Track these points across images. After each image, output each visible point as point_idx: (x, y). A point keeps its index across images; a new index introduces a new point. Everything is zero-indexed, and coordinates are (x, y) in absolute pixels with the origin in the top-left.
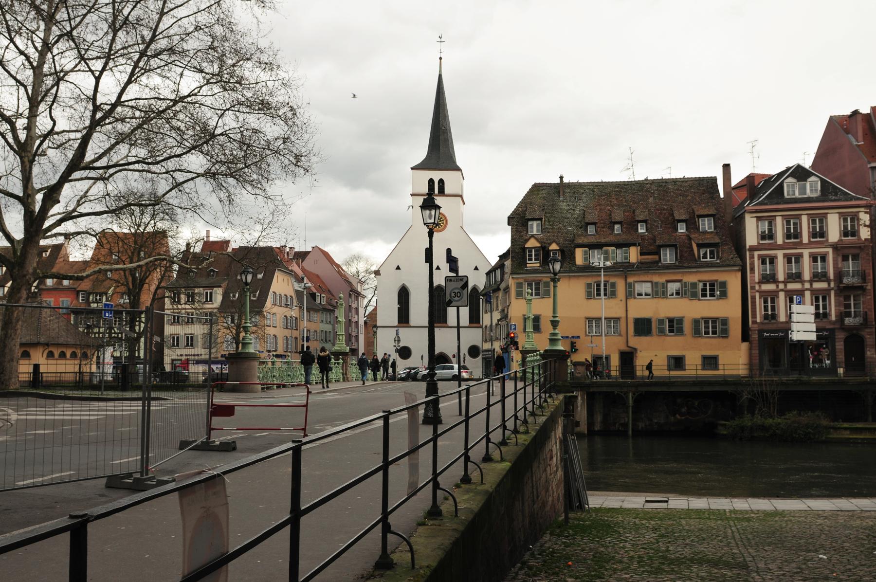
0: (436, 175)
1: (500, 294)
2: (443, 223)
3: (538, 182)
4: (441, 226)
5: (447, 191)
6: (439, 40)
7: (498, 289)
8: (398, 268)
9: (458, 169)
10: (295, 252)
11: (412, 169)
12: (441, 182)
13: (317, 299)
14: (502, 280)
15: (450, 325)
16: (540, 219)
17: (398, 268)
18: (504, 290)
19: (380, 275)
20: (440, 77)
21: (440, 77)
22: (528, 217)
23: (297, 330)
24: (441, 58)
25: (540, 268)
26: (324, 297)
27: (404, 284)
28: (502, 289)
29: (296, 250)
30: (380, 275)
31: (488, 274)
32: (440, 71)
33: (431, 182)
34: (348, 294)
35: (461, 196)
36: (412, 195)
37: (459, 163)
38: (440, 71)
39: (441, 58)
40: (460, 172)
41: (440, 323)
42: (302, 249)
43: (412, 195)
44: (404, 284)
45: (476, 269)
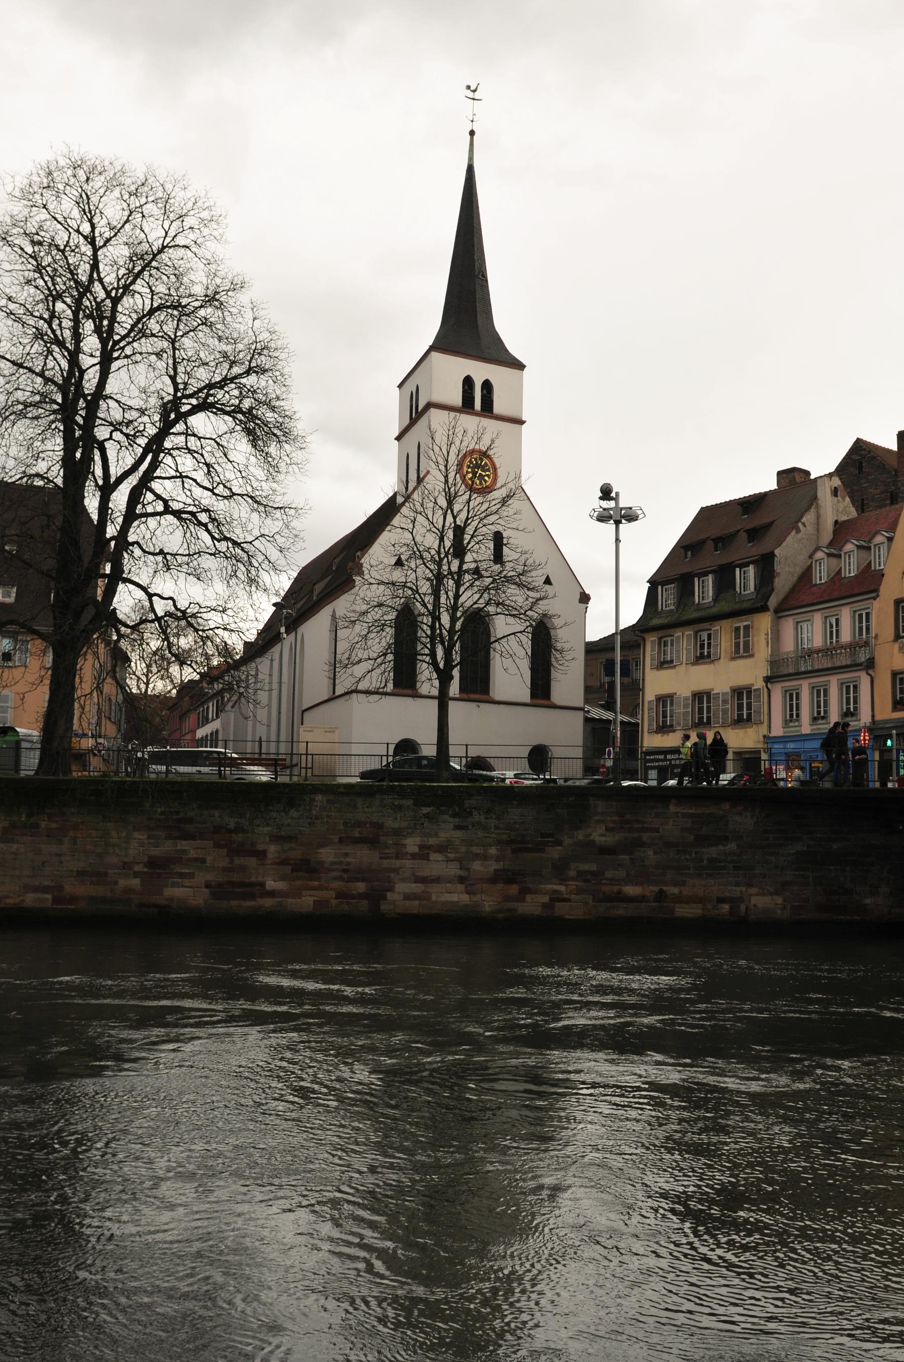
0: (480, 371)
2: (488, 476)
4: (486, 481)
5: (498, 408)
6: (471, 95)
12: (487, 386)
18: (777, 611)
20: (470, 170)
21: (470, 170)
24: (472, 133)
28: (772, 609)
32: (471, 158)
33: (468, 382)
38: (471, 158)
39: (472, 133)
41: (474, 692)
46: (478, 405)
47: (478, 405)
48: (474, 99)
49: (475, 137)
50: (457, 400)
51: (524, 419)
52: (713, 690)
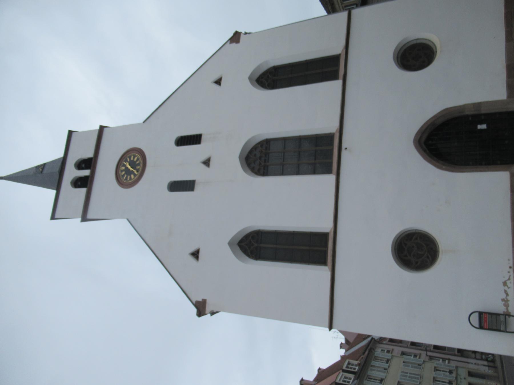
17: (196, 254)
19: (204, 302)
30: (204, 302)
44: (230, 244)
51: (98, 128)
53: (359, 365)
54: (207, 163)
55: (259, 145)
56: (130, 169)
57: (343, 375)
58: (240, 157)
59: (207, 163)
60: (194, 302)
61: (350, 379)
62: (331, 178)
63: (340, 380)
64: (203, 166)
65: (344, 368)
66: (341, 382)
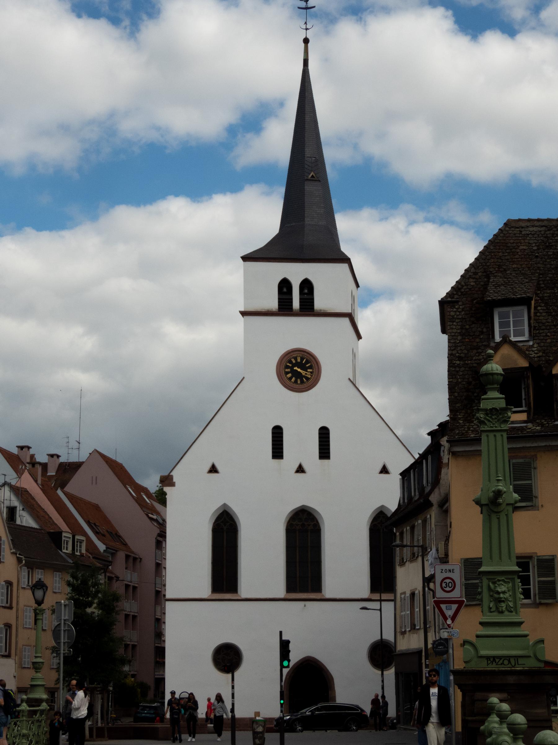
1: (433, 514)
3: (515, 216)
4: (308, 379)
7: (429, 505)
8: (213, 470)
9: (346, 260)
10: (61, 465)
11: (246, 258)
13: (64, 545)
14: (436, 482)
15: (328, 596)
16: (525, 302)
17: (213, 470)
19: (172, 484)
22: (492, 294)
23: (11, 608)
24: (306, 41)
25: (530, 425)
26: (81, 542)
27: (225, 505)
29: (62, 460)
30: (172, 484)
31: (405, 474)
34: (154, 541)
35: (351, 317)
36: (243, 314)
37: (345, 248)
39: (306, 41)
40: (345, 266)
42: (74, 458)
43: (243, 314)
44: (225, 505)
45: (384, 470)
46: (296, 304)
47: (296, 304)
48: (307, 8)
49: (309, 45)
50: (273, 303)
52: (416, 589)
53: (82, 555)
54: (300, 470)
55: (315, 522)
56: (298, 368)
57: (70, 538)
58: (303, 506)
59: (300, 470)
60: (171, 474)
61: (67, 549)
62: (281, 592)
63: (64, 536)
64: (296, 466)
65: (77, 537)
66: (63, 539)
